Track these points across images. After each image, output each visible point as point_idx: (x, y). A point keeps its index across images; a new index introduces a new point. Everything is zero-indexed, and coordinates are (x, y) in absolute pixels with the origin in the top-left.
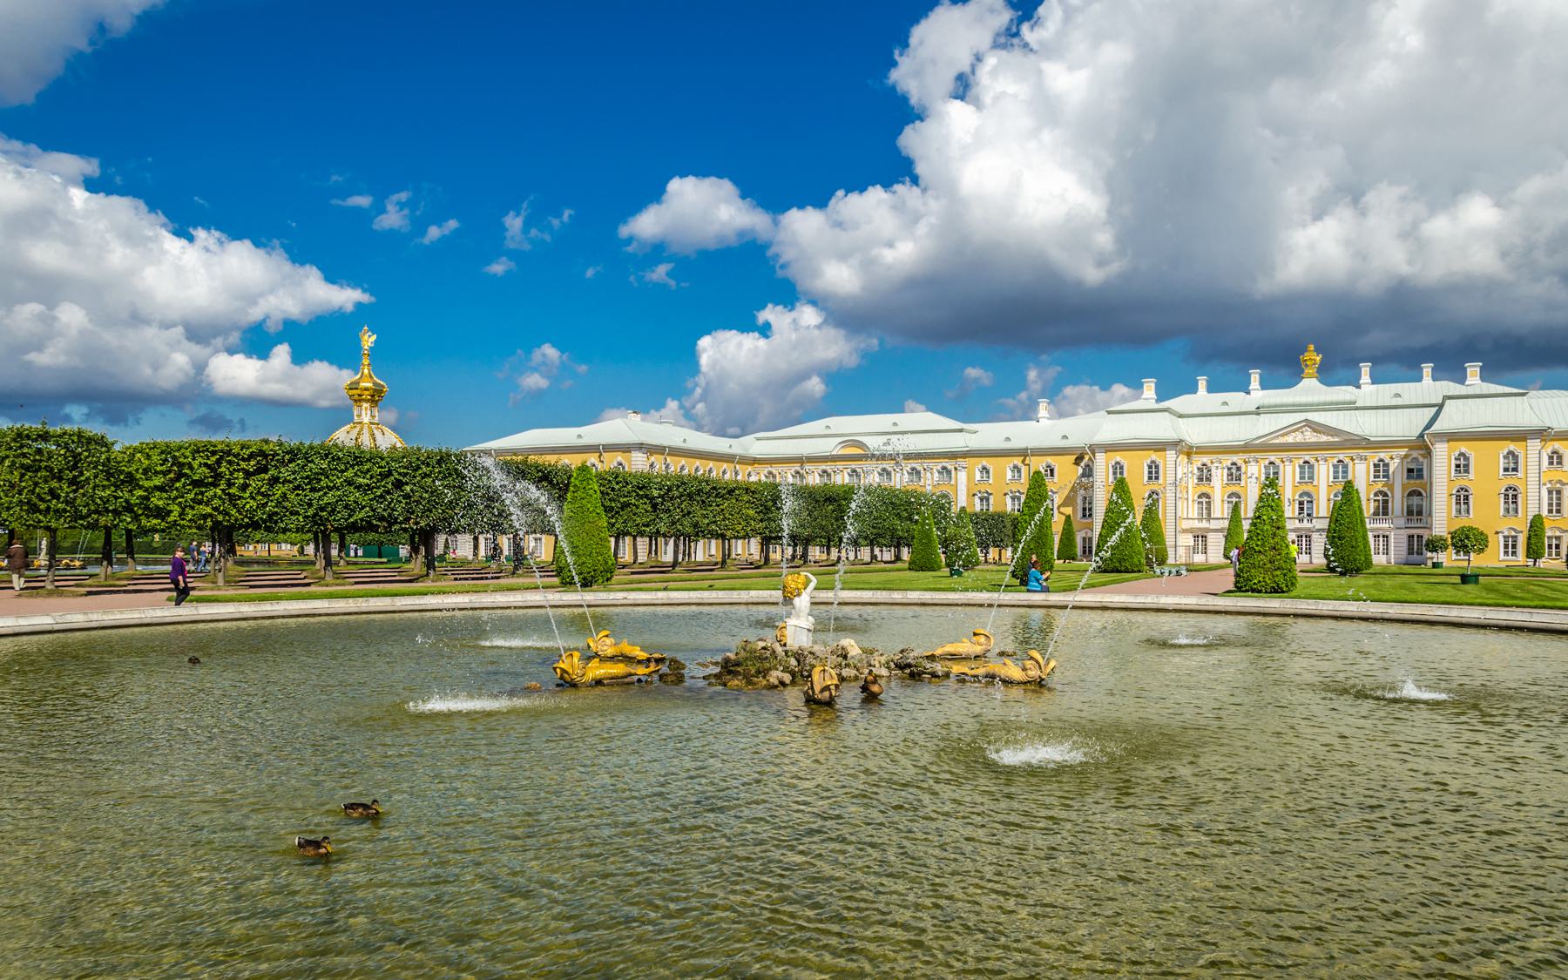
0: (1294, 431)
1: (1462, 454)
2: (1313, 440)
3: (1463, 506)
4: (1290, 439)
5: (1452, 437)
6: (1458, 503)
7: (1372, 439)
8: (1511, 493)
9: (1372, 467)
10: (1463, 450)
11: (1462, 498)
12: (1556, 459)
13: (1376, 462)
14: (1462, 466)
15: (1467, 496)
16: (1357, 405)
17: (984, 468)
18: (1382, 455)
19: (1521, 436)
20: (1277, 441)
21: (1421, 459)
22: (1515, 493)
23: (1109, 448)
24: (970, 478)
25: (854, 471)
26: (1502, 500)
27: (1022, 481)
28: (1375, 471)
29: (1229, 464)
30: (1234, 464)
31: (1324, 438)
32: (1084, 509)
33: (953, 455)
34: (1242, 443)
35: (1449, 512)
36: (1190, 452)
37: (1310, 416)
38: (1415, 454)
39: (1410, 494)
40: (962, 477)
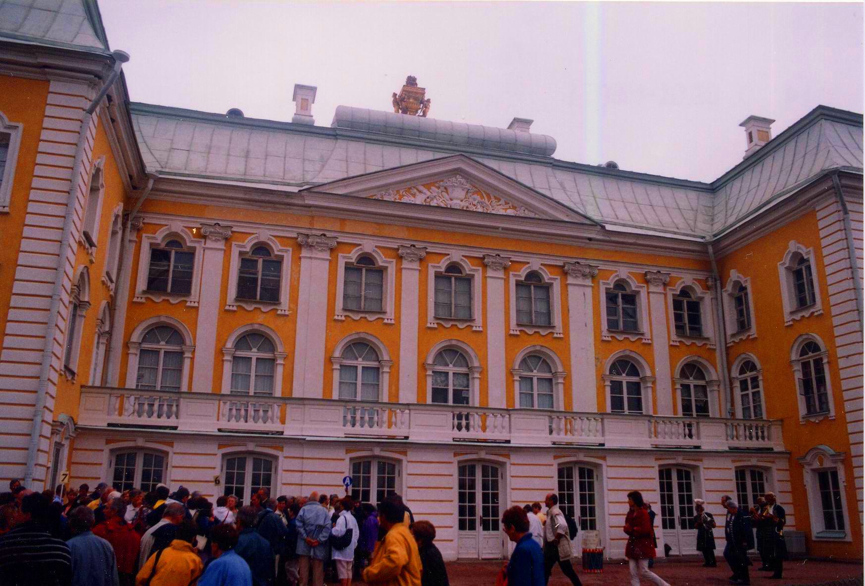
0: (428, 186)
7: (609, 227)
18: (623, 272)
29: (248, 245)
30: (262, 248)
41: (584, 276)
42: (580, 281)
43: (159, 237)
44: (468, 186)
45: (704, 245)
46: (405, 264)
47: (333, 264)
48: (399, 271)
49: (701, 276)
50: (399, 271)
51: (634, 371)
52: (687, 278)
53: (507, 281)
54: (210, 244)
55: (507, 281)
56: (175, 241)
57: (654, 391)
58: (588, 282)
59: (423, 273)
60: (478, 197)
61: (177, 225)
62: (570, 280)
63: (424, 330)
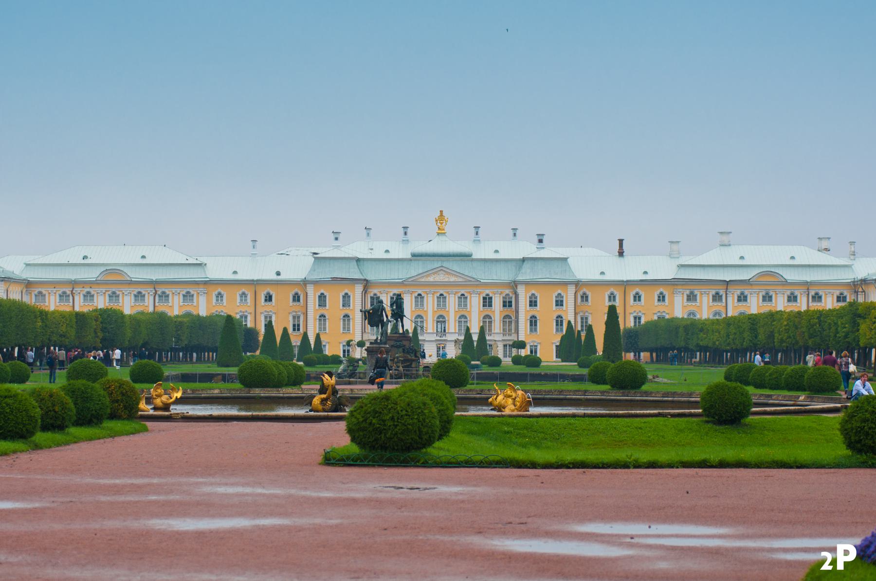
0: (434, 274)
1: (533, 294)
2: (446, 280)
3: (533, 327)
4: (431, 279)
5: (527, 283)
6: (531, 325)
7: (482, 281)
8: (559, 319)
9: (482, 299)
10: (533, 292)
11: (533, 322)
12: (585, 297)
13: (484, 296)
14: (533, 303)
15: (536, 321)
16: (474, 257)
17: (219, 294)
18: (487, 292)
19: (565, 284)
20: (423, 280)
21: (511, 295)
22: (561, 319)
23: (316, 283)
24: (209, 301)
25: (114, 293)
26: (555, 324)
27: (249, 304)
28: (484, 302)
31: (452, 279)
32: (294, 325)
33: (196, 283)
34: (401, 281)
35: (526, 331)
36: (367, 284)
37: (445, 264)
38: (507, 291)
39: (505, 317)
40: (202, 300)
41: (476, 294)
42: (475, 295)
43: (372, 295)
44: (445, 273)
45: (510, 283)
46: (429, 295)
47: (411, 297)
48: (427, 297)
49: (512, 290)
50: (427, 297)
51: (490, 318)
52: (507, 291)
53: (455, 297)
54: (383, 295)
55: (455, 297)
56: (375, 294)
57: (494, 323)
58: (478, 295)
59: (433, 297)
60: (447, 276)
61: (376, 291)
62: (472, 295)
63: (434, 312)
